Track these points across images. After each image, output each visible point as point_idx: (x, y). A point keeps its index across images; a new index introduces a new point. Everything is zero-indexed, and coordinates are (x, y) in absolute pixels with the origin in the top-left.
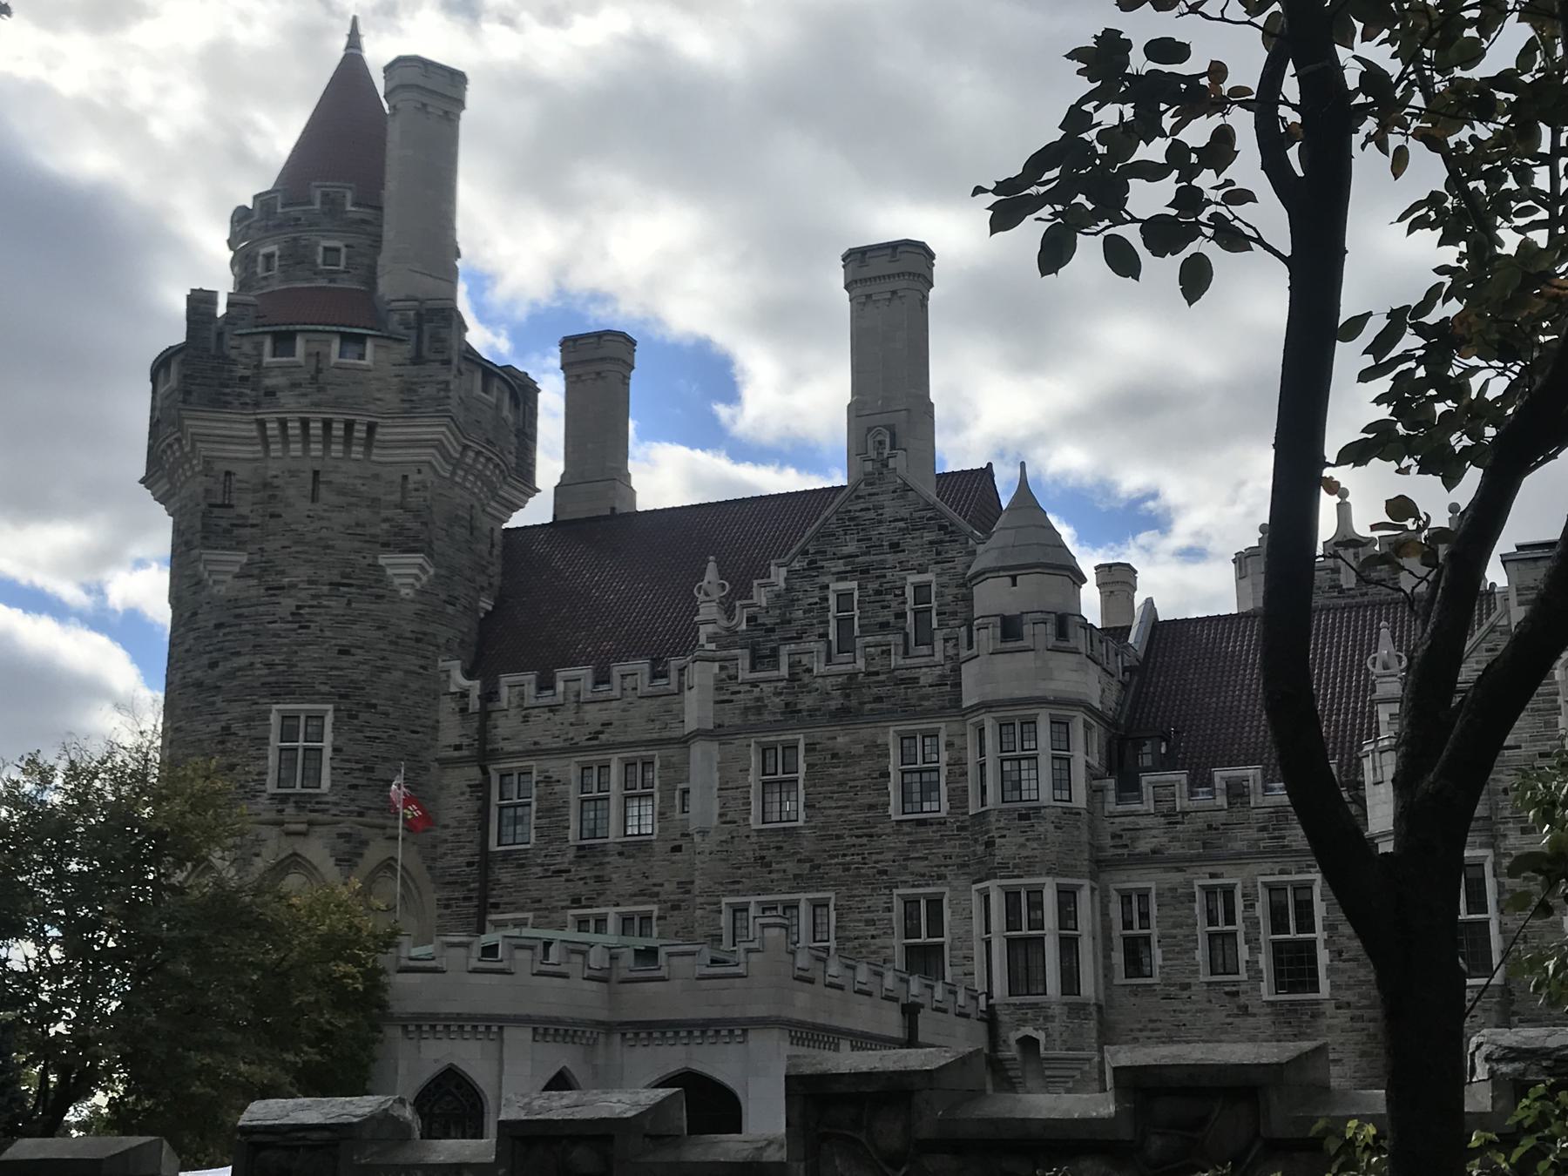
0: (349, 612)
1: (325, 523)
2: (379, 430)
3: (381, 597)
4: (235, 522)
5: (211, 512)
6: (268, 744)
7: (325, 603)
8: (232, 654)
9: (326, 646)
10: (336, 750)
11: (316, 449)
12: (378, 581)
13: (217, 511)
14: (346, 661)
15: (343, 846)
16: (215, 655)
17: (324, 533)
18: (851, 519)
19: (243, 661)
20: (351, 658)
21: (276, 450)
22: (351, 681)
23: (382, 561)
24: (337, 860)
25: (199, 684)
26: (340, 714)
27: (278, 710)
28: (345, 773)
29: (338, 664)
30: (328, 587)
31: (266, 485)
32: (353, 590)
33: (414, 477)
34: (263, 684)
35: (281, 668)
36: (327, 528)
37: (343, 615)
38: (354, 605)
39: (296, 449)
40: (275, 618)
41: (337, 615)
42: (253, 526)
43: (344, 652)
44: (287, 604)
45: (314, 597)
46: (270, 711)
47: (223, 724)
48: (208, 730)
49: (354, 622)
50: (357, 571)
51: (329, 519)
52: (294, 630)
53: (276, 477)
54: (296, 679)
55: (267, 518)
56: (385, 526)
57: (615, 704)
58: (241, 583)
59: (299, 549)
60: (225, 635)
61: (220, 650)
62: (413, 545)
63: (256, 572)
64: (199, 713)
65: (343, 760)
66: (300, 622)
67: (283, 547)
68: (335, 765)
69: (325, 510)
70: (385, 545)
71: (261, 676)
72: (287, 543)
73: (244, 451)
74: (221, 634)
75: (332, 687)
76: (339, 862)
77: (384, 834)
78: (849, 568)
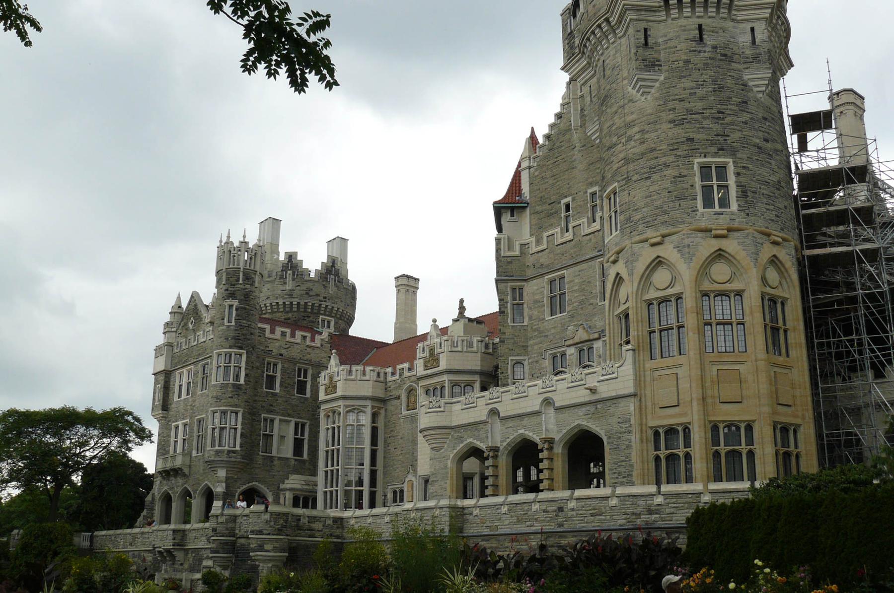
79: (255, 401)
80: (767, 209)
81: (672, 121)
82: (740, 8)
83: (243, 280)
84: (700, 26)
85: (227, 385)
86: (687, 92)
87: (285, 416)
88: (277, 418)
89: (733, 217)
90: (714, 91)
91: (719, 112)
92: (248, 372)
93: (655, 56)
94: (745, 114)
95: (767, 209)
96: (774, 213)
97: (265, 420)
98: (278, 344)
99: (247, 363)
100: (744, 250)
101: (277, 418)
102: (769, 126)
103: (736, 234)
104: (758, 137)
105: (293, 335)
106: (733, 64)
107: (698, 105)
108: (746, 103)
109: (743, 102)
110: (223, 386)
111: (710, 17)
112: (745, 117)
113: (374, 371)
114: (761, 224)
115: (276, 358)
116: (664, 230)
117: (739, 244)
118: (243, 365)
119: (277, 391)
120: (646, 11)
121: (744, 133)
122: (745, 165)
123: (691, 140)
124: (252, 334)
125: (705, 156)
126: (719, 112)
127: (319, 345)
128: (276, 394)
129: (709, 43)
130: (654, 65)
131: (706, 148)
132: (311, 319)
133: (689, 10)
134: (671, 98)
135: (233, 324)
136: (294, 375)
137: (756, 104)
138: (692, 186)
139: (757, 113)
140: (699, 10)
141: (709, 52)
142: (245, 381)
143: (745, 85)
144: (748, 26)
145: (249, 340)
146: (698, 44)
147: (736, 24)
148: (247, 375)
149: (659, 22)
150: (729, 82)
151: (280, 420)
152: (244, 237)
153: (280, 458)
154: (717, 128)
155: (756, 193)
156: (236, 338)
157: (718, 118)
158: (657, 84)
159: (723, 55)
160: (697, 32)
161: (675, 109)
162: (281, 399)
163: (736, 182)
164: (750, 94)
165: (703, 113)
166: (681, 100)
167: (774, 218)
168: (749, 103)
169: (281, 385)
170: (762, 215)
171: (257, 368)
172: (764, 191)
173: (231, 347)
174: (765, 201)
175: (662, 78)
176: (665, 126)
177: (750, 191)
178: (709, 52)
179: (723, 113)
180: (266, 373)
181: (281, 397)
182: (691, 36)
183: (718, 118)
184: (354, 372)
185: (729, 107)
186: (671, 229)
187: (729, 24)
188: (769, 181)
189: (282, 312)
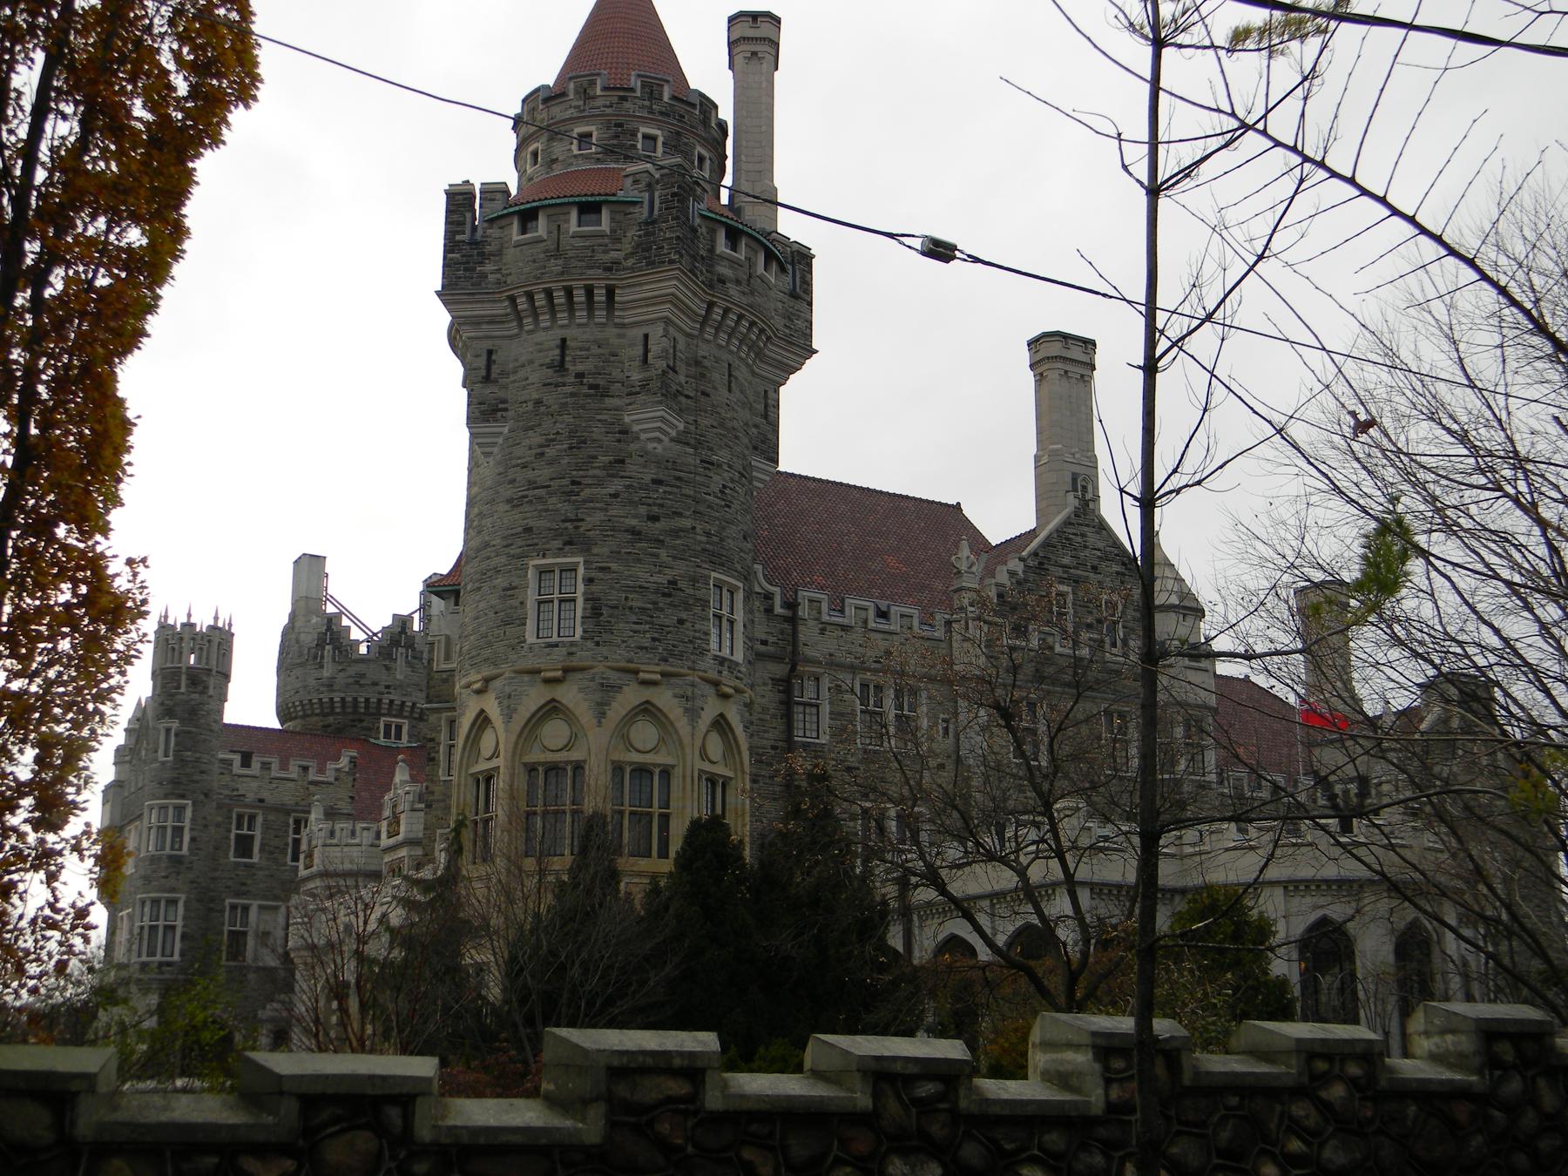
8: (674, 513)
18: (1067, 539)
25: (634, 532)
31: (697, 363)
40: (709, 490)
42: (688, 397)
44: (717, 480)
47: (670, 578)
48: (652, 579)
57: (895, 637)
58: (679, 447)
60: (665, 492)
61: (661, 506)
63: (693, 442)
64: (639, 561)
71: (701, 542)
72: (715, 424)
78: (1065, 576)
79: (213, 879)
81: (509, 501)
82: (627, 306)
83: (187, 686)
84: (564, 341)
85: (159, 858)
86: (534, 452)
87: (267, 899)
88: (255, 905)
89: (573, 649)
90: (571, 448)
91: (574, 483)
92: (195, 833)
93: (501, 394)
94: (616, 481)
96: (648, 635)
97: (234, 907)
98: (254, 784)
99: (193, 820)
100: (585, 700)
101: (255, 905)
103: (579, 675)
104: (635, 516)
105: (284, 767)
106: (607, 400)
107: (543, 473)
108: (622, 462)
109: (617, 461)
110: (153, 860)
111: (580, 325)
112: (616, 485)
113: (368, 829)
114: (619, 656)
115: (253, 807)
116: (487, 671)
117: (581, 690)
118: (187, 824)
119: (256, 859)
120: (488, 323)
121: (611, 513)
123: (528, 530)
124: (202, 772)
125: (544, 556)
126: (574, 483)
127: (331, 779)
128: (252, 866)
129: (571, 368)
130: (496, 410)
131: (548, 543)
132: (365, 724)
133: (530, 320)
134: (514, 462)
135: (171, 758)
136: (287, 832)
137: (641, 460)
138: (522, 603)
140: (562, 316)
141: (572, 384)
142: (189, 849)
143: (625, 432)
144: (638, 333)
145: (197, 782)
146: (556, 371)
147: (621, 331)
148: (193, 840)
149: (511, 337)
150: (597, 431)
151: (261, 907)
152: (189, 615)
153: (259, 969)
154: (566, 509)
155: (617, 607)
156: (175, 782)
157: (571, 493)
158: (500, 440)
159: (591, 387)
160: (557, 352)
161: (515, 480)
162: (261, 873)
163: (584, 594)
164: (633, 447)
165: (549, 486)
166: (524, 466)
168: (627, 461)
169: (262, 850)
170: (623, 642)
171: (218, 825)
172: (635, 604)
173: (166, 797)
174: (634, 618)
175: (506, 430)
176: (503, 507)
177: (606, 605)
178: (572, 384)
179: (579, 483)
180: (234, 832)
181: (261, 869)
182: (547, 360)
183: (571, 493)
184: (338, 834)
185: (591, 473)
186: (492, 671)
187: (611, 332)
189: (317, 715)
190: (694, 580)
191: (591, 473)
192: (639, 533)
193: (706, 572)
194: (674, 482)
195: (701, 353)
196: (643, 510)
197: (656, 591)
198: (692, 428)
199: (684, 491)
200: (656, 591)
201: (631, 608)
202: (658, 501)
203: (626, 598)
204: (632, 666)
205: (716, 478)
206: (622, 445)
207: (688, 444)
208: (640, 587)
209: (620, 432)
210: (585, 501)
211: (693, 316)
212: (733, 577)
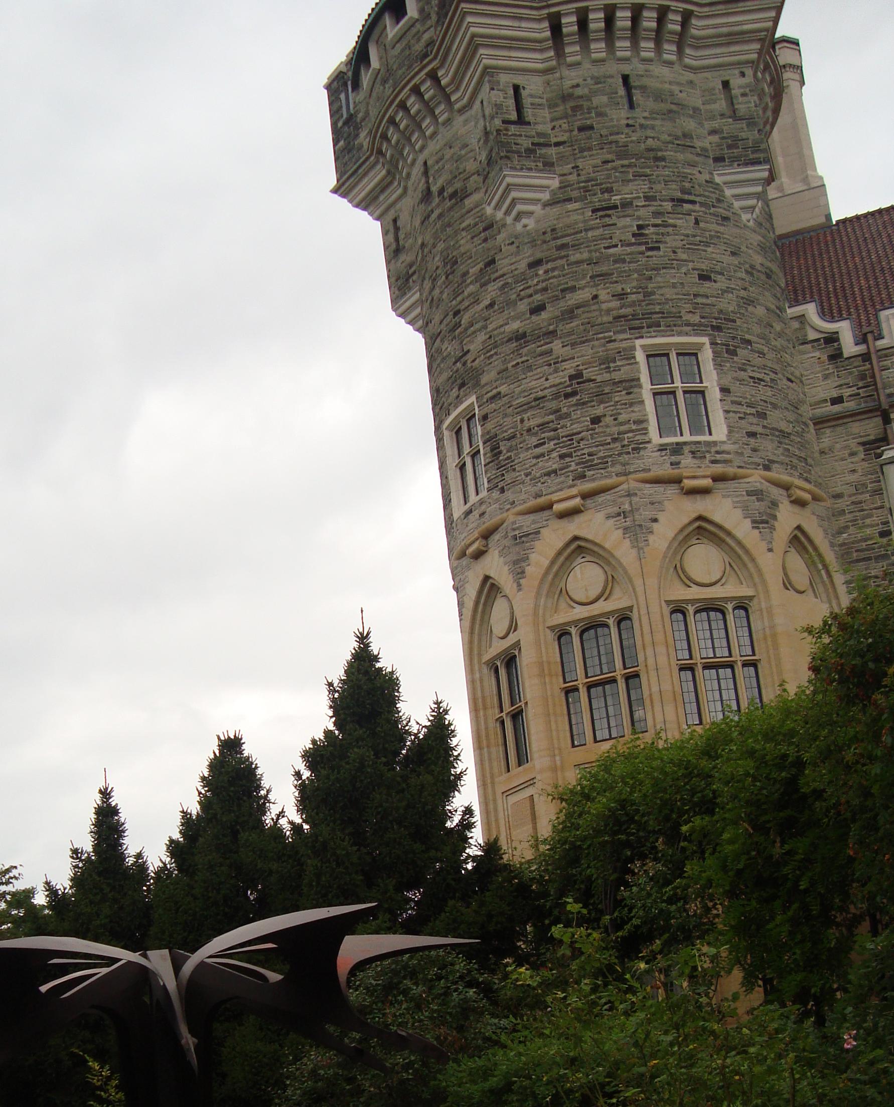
0: (698, 232)
1: (649, 133)
2: (694, 21)
3: (726, 219)
4: (536, 140)
5: (507, 130)
6: (640, 386)
7: (671, 221)
8: (563, 291)
9: (684, 270)
10: (724, 390)
11: (623, 45)
12: (719, 201)
13: (513, 129)
14: (707, 287)
15: (757, 506)
16: (538, 297)
17: (650, 142)
19: (584, 295)
20: (715, 286)
21: (573, 54)
22: (721, 312)
23: (718, 179)
24: (754, 522)
25: (520, 337)
26: (719, 348)
27: (642, 346)
28: (740, 418)
29: (702, 291)
30: (671, 204)
32: (697, 207)
33: (737, 82)
34: (617, 318)
35: (633, 297)
36: (653, 138)
37: (694, 236)
38: (702, 225)
39: (598, 48)
41: (687, 236)
42: (557, 144)
43: (704, 277)
44: (625, 225)
45: (657, 214)
46: (633, 348)
48: (547, 384)
49: (707, 244)
50: (697, 187)
51: (653, 128)
52: (642, 253)
53: (578, 86)
54: (657, 308)
55: (576, 132)
56: (715, 138)
58: (556, 210)
59: (626, 162)
61: (545, 289)
62: (751, 157)
63: (575, 194)
64: (530, 368)
65: (733, 402)
66: (647, 243)
67: (606, 162)
68: (726, 408)
69: (645, 118)
70: (719, 160)
71: (608, 311)
72: (610, 157)
73: (534, 60)
74: (541, 272)
75: (702, 317)
76: (757, 523)
77: (789, 496)
80: (537, 457)
95: (537, 457)
96: (555, 454)
102: (546, 272)
108: (493, 261)
112: (492, 290)
121: (490, 327)
122: (495, 391)
137: (513, 248)
139: (513, 267)
155: (514, 437)
167: (555, 466)
170: (527, 475)
172: (533, 423)
174: (534, 441)
185: (466, 293)
188: (541, 394)
190: (606, 362)
191: (466, 293)
192: (524, 335)
193: (624, 344)
194: (556, 254)
195: (568, 83)
196: (523, 306)
197: (556, 396)
198: (573, 178)
199: (572, 259)
200: (556, 396)
201: (529, 430)
202: (539, 287)
203: (522, 421)
204: (541, 501)
205: (622, 222)
206: (490, 244)
207: (569, 200)
208: (536, 399)
209: (485, 230)
210: (466, 329)
211: (537, 46)
212: (680, 334)
